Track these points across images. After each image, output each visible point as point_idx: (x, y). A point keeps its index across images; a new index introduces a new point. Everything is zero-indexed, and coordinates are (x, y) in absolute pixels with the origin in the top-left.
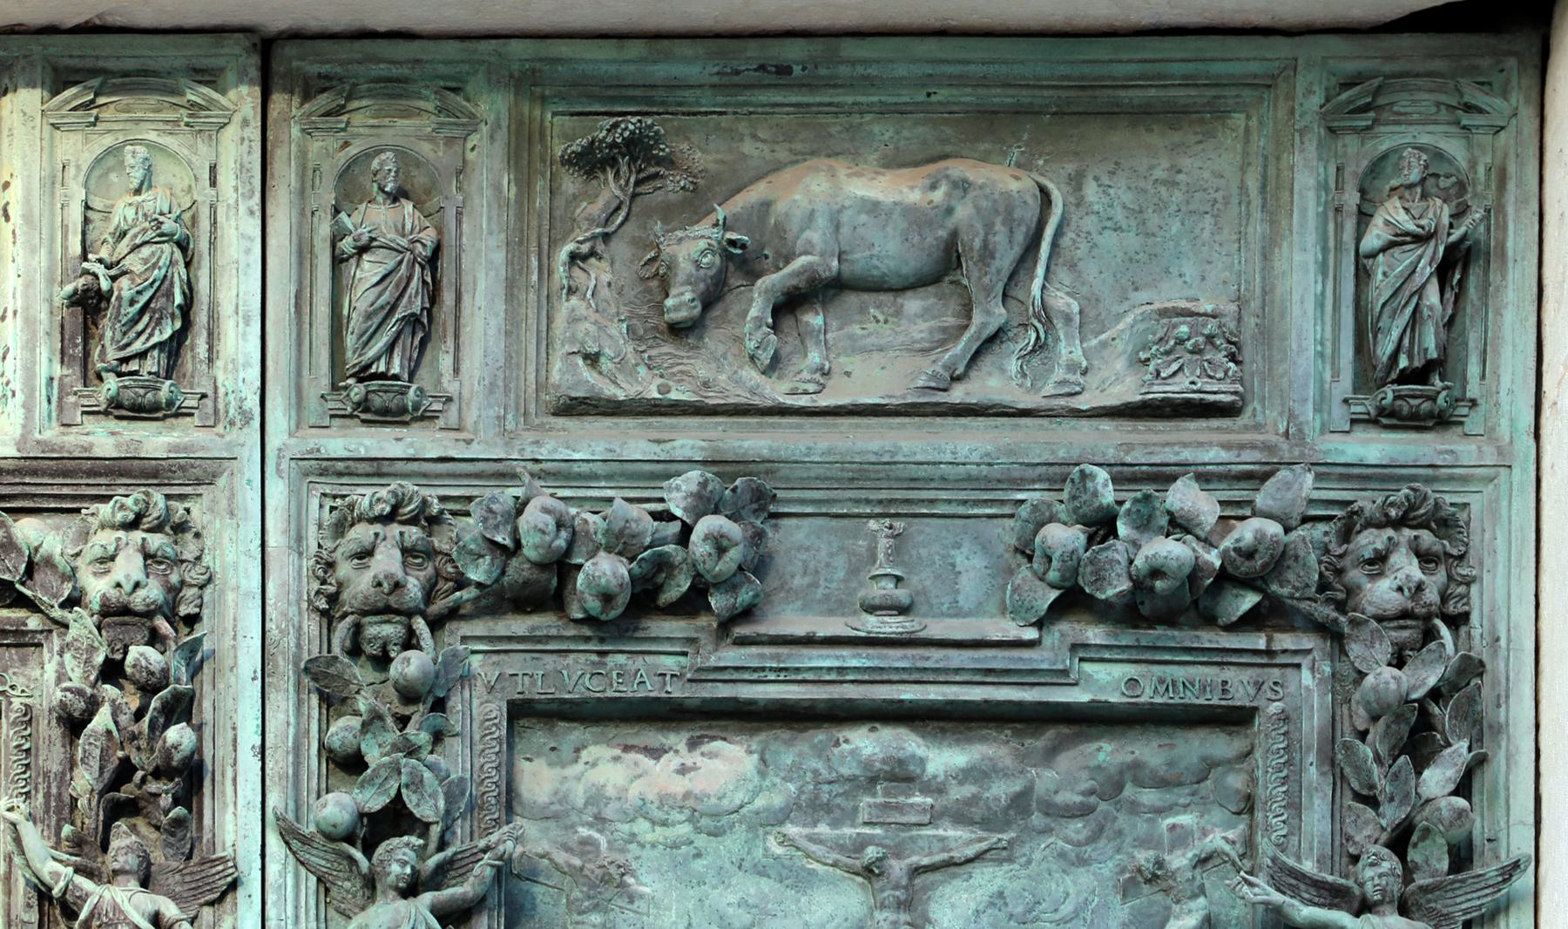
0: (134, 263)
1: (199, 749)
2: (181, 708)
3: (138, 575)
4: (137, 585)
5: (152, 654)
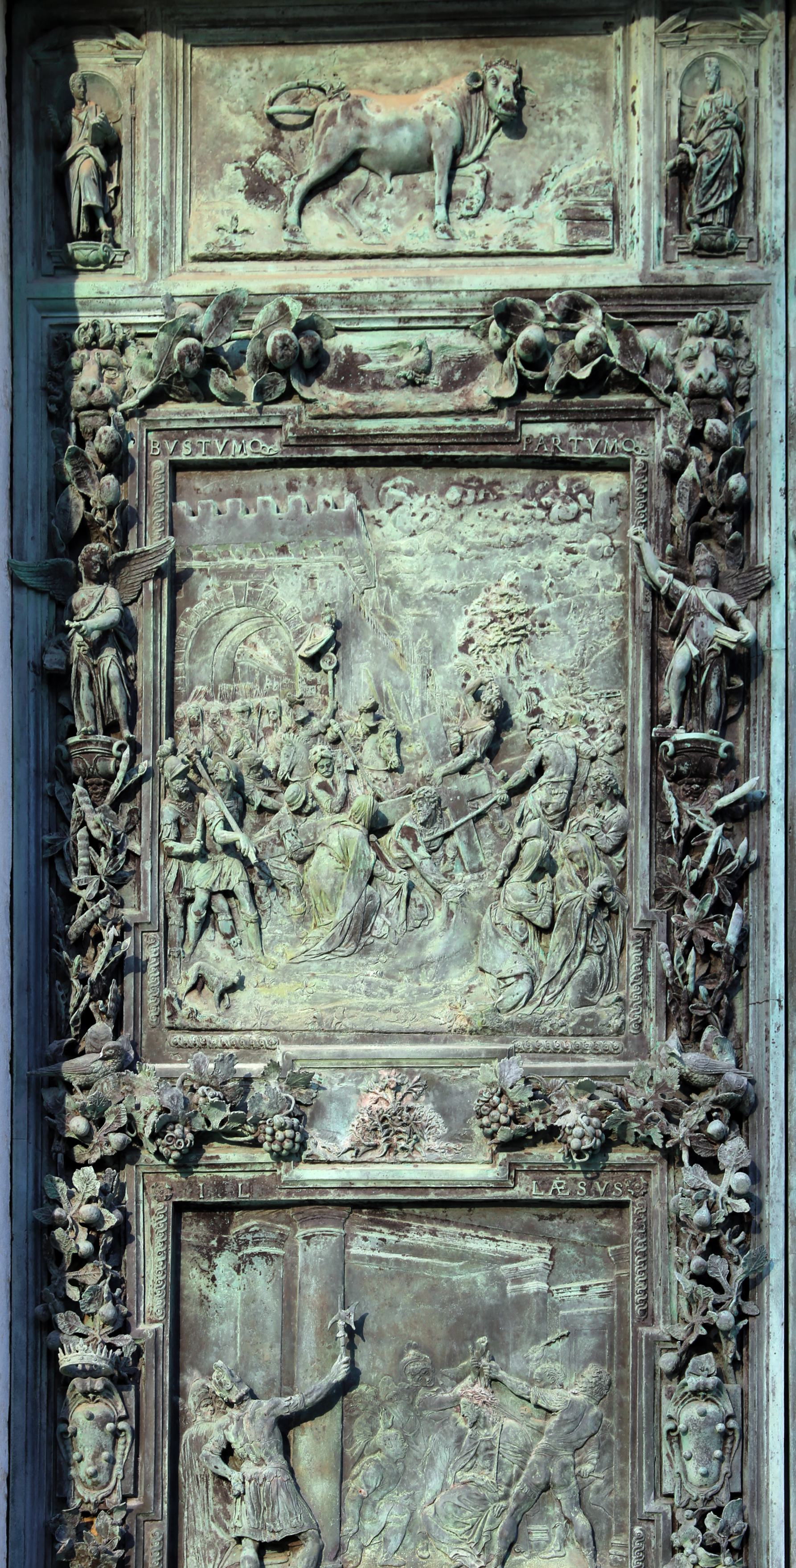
0: (709, 144)
1: (747, 492)
2: (737, 463)
3: (712, 369)
4: (711, 376)
5: (719, 423)
